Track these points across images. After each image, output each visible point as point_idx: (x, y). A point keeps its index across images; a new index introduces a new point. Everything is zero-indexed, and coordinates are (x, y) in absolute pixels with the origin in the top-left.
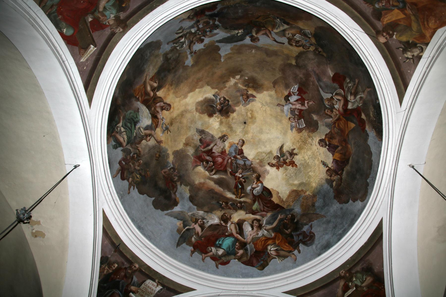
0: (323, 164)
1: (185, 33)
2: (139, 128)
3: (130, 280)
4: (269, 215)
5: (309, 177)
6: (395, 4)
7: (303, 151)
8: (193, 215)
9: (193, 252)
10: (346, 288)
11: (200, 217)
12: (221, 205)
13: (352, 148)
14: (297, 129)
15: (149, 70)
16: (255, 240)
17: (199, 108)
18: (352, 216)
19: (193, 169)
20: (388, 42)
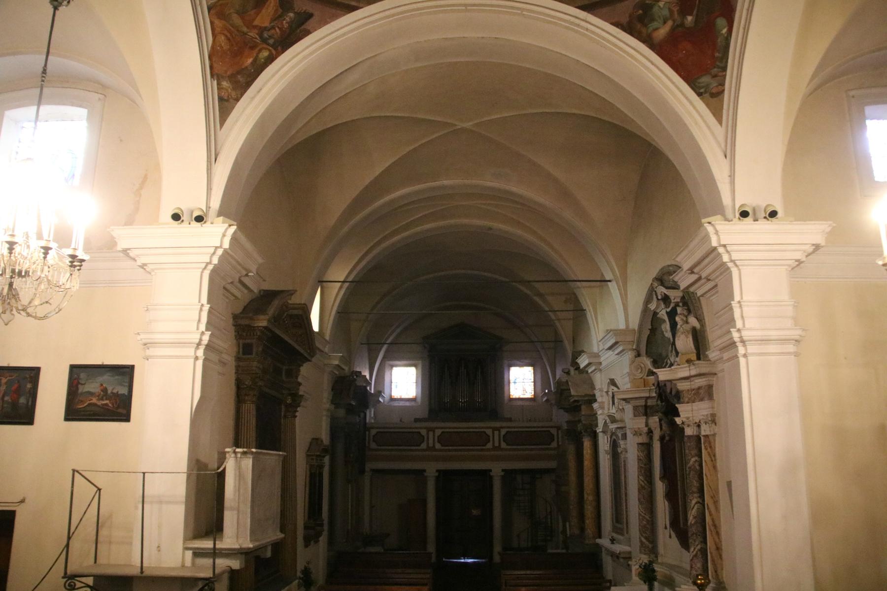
6: (273, 31)
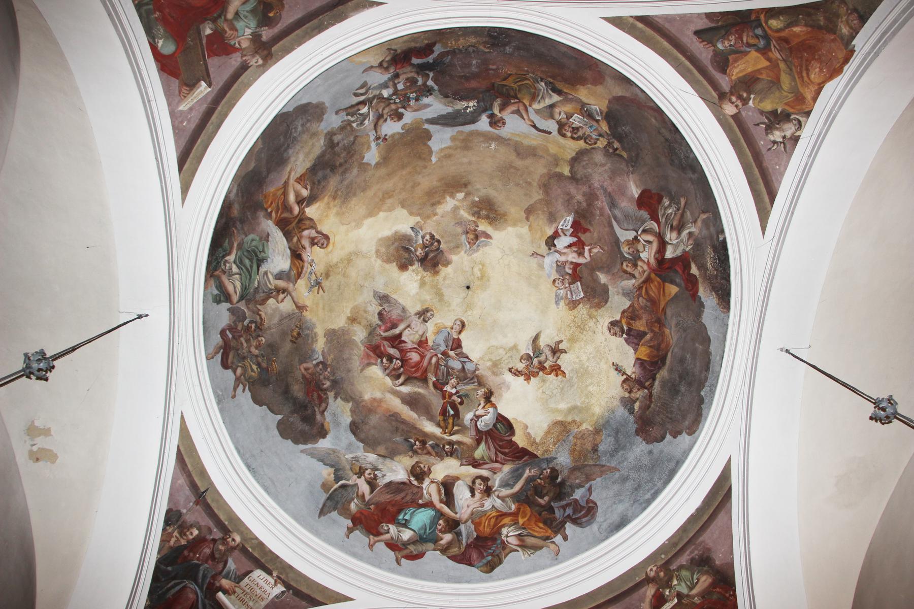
0: (616, 369)
1: (371, 96)
2: (266, 273)
3: (221, 566)
4: (507, 468)
5: (589, 395)
6: (752, 41)
7: (577, 345)
8: (356, 459)
9: (350, 530)
10: (659, 600)
11: (369, 466)
12: (412, 446)
13: (672, 334)
14: (567, 302)
15: (296, 161)
16: (476, 518)
17: (383, 250)
18: (672, 465)
19: (362, 370)
20: (739, 112)
